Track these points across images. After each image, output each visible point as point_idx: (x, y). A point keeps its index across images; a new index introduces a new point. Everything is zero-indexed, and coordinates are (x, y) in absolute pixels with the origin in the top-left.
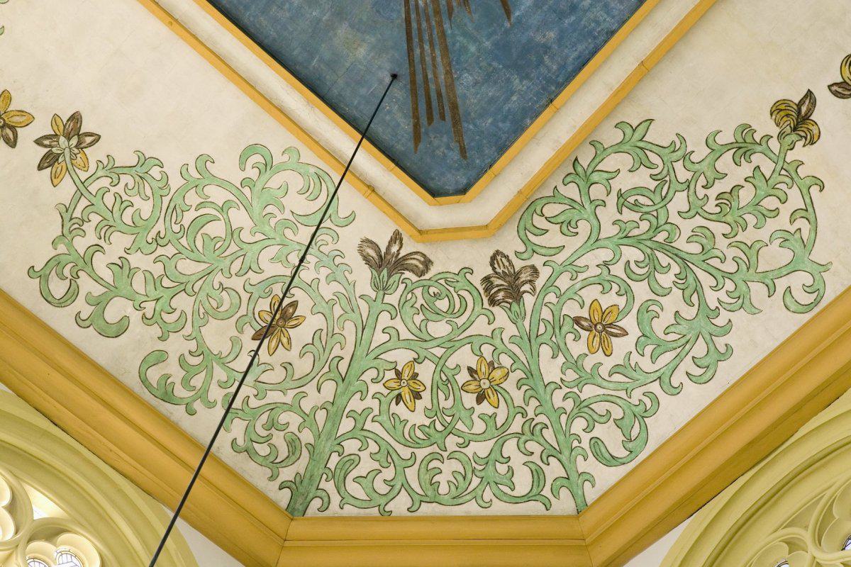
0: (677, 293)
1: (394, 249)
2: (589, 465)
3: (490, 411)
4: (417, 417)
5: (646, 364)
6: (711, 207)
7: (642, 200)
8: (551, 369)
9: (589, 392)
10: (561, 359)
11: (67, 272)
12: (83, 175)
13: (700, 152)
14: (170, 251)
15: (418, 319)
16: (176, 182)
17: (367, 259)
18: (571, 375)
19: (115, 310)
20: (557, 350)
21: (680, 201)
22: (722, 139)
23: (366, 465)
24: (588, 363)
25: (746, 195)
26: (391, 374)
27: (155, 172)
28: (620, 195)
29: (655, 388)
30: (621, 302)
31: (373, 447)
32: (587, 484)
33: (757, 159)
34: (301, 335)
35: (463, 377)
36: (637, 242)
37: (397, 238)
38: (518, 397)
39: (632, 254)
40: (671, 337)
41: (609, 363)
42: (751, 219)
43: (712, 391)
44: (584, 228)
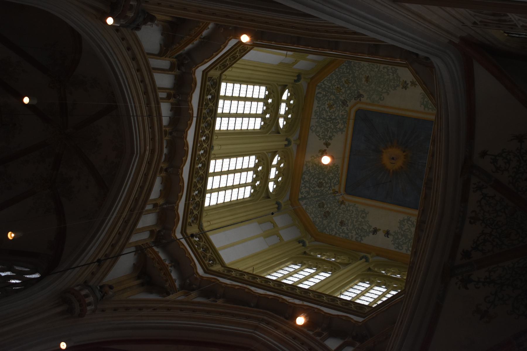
0: (325, 117)
1: (360, 99)
2: (320, 91)
3: (335, 87)
4: (343, 79)
5: (322, 107)
6: (329, 129)
7: (337, 124)
8: (332, 97)
9: (326, 98)
10: (332, 99)
11: (394, 71)
12: (401, 83)
13: (334, 134)
14: (385, 80)
15: (352, 91)
16: (390, 89)
17: (362, 95)
18: (330, 98)
19: (386, 70)
20: (333, 100)
21: (332, 127)
22: (333, 137)
23: (345, 70)
24: (329, 101)
25: (326, 133)
26: (350, 82)
27: (393, 89)
28: (339, 123)
29: (319, 105)
30: (330, 111)
31: (345, 72)
32: (318, 88)
33: (328, 137)
34: (364, 80)
35: (342, 88)
36: (334, 119)
37: (360, 100)
38: (334, 91)
39: (333, 117)
40: (322, 112)
41: (327, 103)
42: (324, 131)
43: (314, 110)
44: (340, 116)
